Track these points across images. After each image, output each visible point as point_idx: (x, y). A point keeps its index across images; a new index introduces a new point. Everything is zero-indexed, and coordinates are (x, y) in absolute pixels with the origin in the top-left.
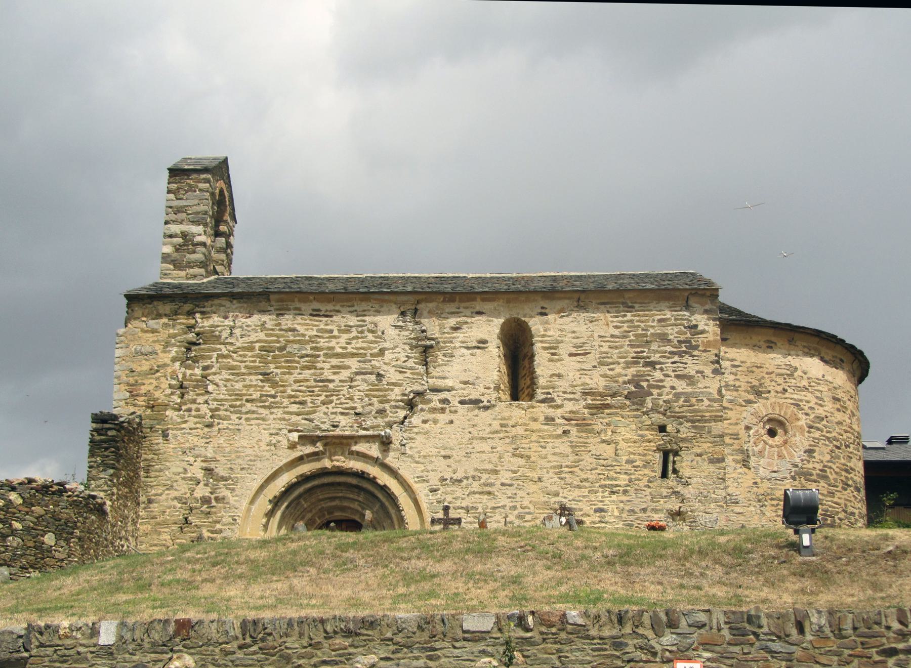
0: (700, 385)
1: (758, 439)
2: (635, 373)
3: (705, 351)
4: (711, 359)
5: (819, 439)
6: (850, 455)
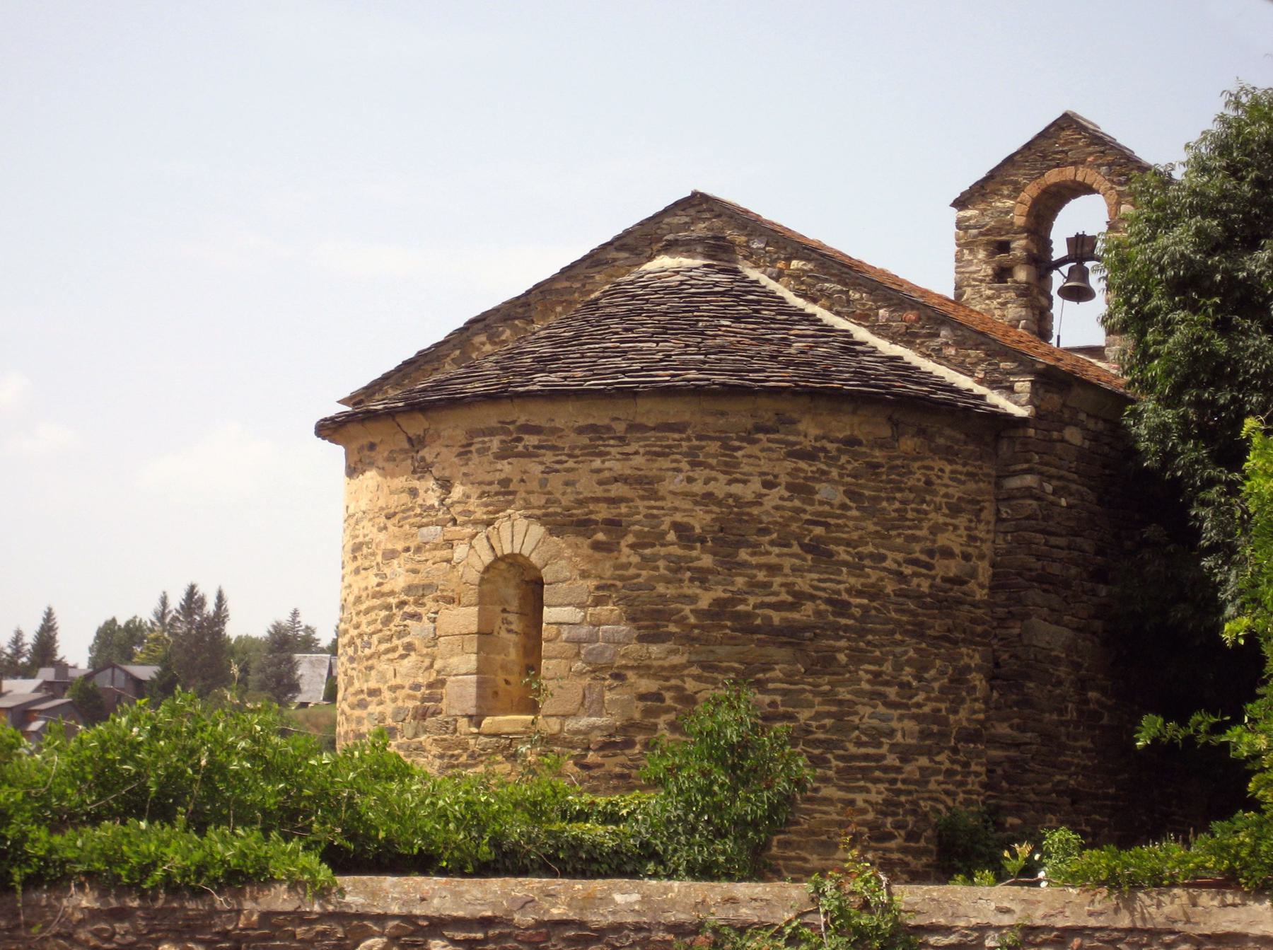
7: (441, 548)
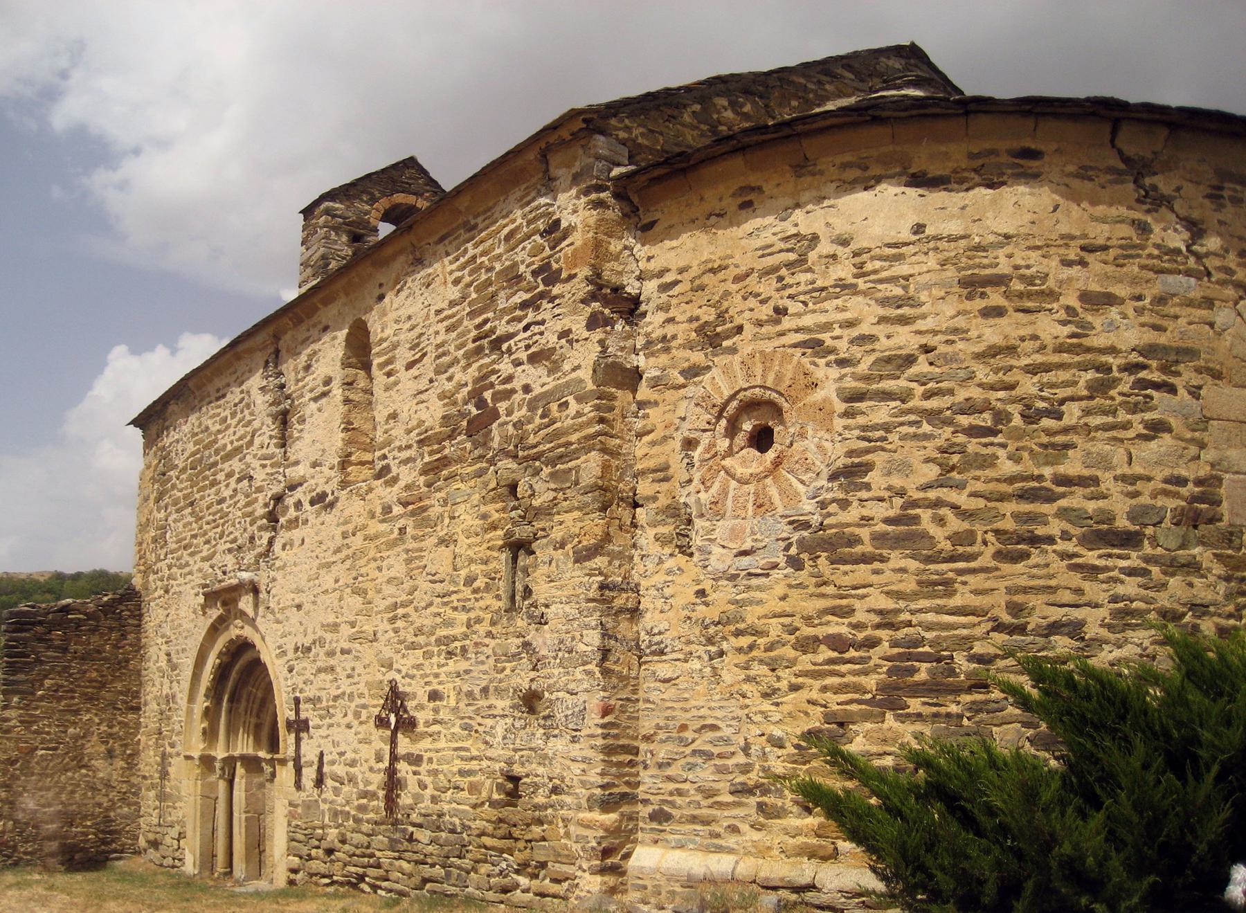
0: (567, 367)
1: (710, 469)
2: (476, 374)
3: (571, 277)
4: (581, 295)
5: (887, 428)
6: (1060, 439)
7: (1199, 307)
